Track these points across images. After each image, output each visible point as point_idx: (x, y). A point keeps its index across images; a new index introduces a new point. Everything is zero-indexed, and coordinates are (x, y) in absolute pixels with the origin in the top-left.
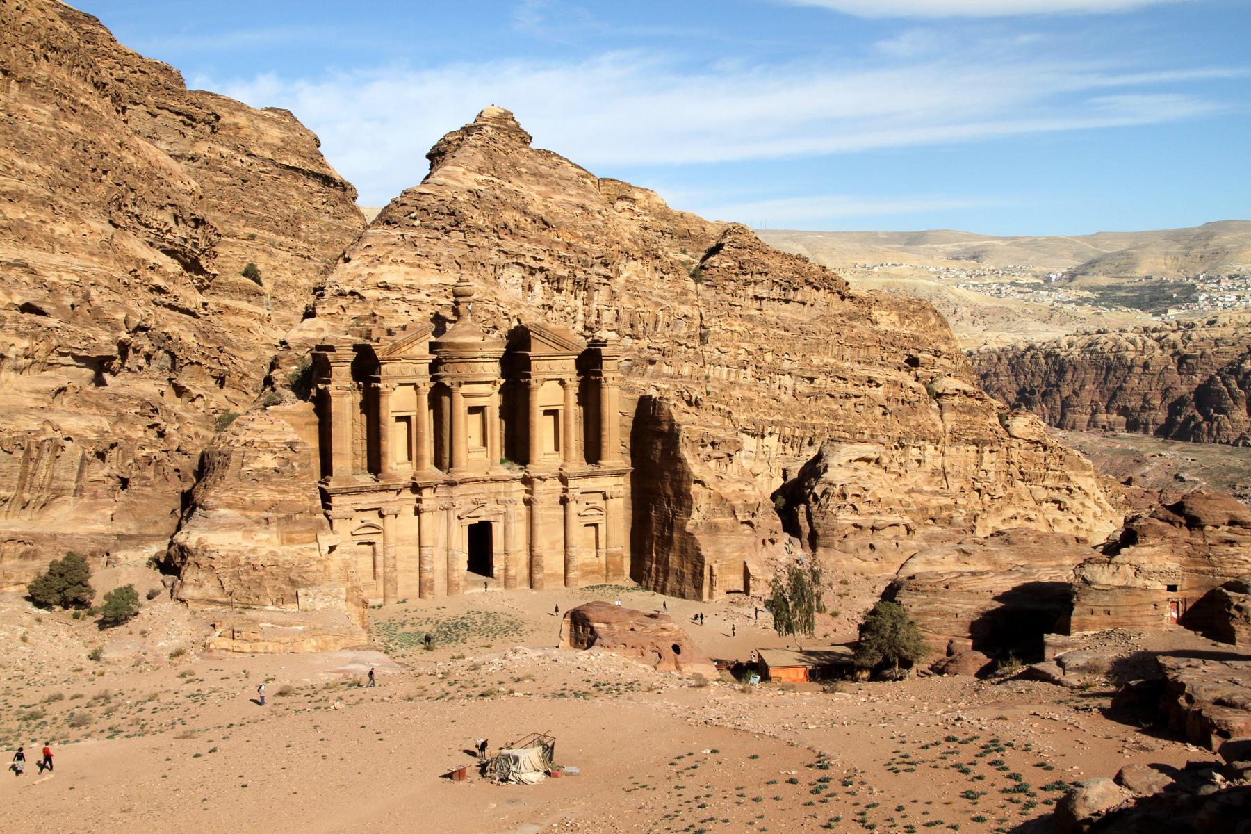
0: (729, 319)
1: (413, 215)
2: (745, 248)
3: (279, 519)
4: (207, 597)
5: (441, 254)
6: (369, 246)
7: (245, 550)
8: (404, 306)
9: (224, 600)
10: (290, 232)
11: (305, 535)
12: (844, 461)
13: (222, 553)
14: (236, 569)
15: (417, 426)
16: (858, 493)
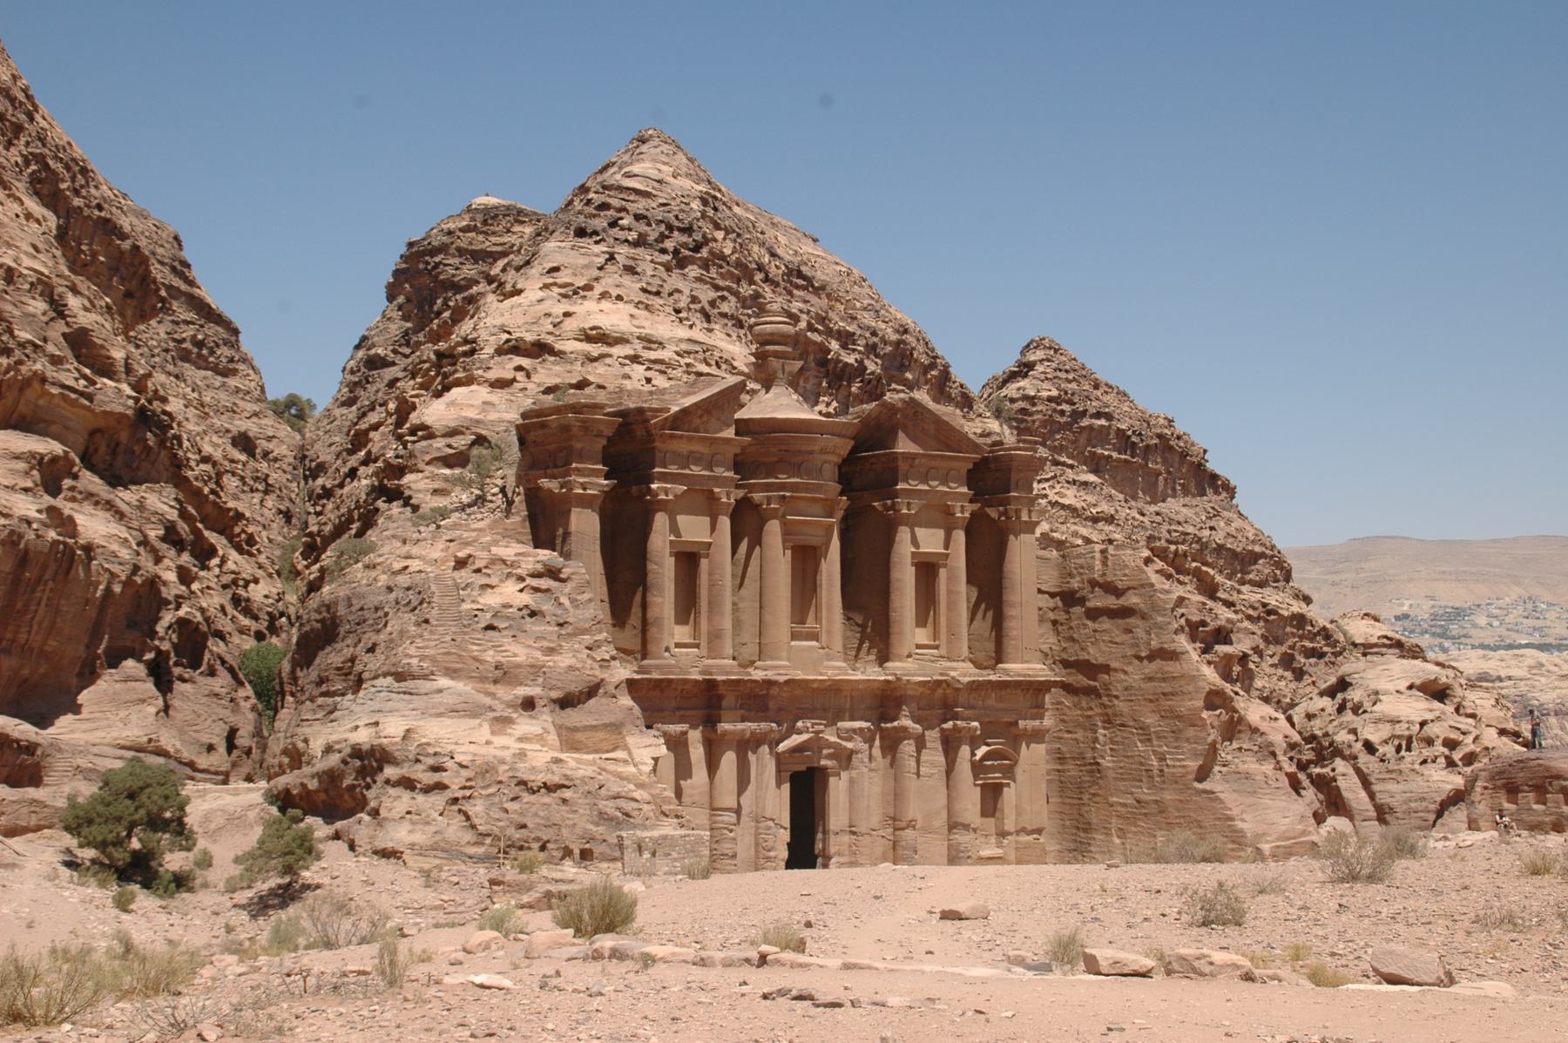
0: (1058, 486)
1: (624, 222)
2: (1067, 371)
3: (554, 701)
4: (442, 844)
5: (679, 291)
6: (556, 269)
7: (507, 754)
8: (638, 371)
9: (480, 850)
10: (170, 368)
11: (600, 735)
12: (1403, 685)
13: (459, 758)
14: (491, 790)
15: (710, 574)
16: (1454, 735)
